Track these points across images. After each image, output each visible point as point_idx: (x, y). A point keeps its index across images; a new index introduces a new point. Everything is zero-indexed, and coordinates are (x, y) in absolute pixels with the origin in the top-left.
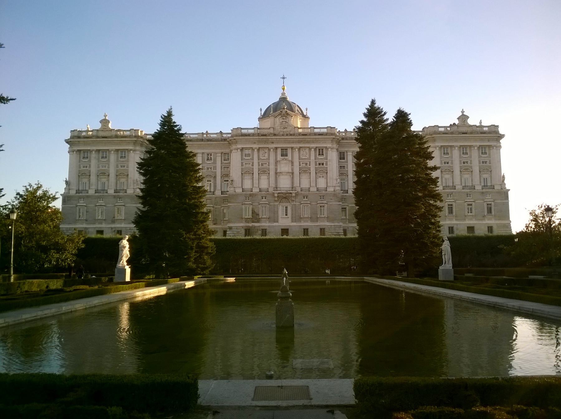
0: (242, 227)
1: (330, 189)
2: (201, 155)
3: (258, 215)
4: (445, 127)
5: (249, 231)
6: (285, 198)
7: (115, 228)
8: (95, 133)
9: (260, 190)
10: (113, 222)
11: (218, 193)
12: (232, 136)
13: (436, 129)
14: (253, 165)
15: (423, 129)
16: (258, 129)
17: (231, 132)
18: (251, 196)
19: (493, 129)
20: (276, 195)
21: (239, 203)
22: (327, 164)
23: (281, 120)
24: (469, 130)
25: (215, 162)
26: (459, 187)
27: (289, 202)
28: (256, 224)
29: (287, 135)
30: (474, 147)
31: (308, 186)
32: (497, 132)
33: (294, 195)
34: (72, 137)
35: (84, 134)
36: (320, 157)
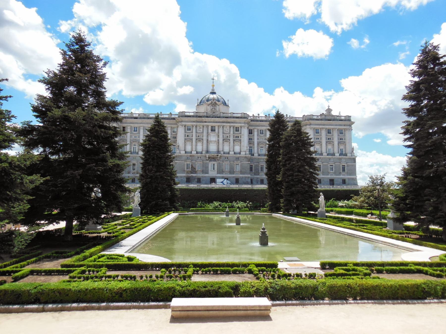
1: (243, 153)
3: (195, 169)
4: (318, 116)
5: (189, 180)
6: (214, 158)
9: (197, 153)
12: (179, 117)
13: (311, 117)
14: (192, 136)
15: (303, 116)
16: (196, 112)
17: (178, 114)
18: (190, 156)
19: (347, 118)
20: (207, 156)
22: (241, 137)
23: (212, 108)
24: (333, 118)
26: (325, 154)
27: (216, 161)
28: (194, 175)
29: (215, 117)
30: (335, 129)
32: (349, 120)
33: (219, 156)
36: (236, 132)
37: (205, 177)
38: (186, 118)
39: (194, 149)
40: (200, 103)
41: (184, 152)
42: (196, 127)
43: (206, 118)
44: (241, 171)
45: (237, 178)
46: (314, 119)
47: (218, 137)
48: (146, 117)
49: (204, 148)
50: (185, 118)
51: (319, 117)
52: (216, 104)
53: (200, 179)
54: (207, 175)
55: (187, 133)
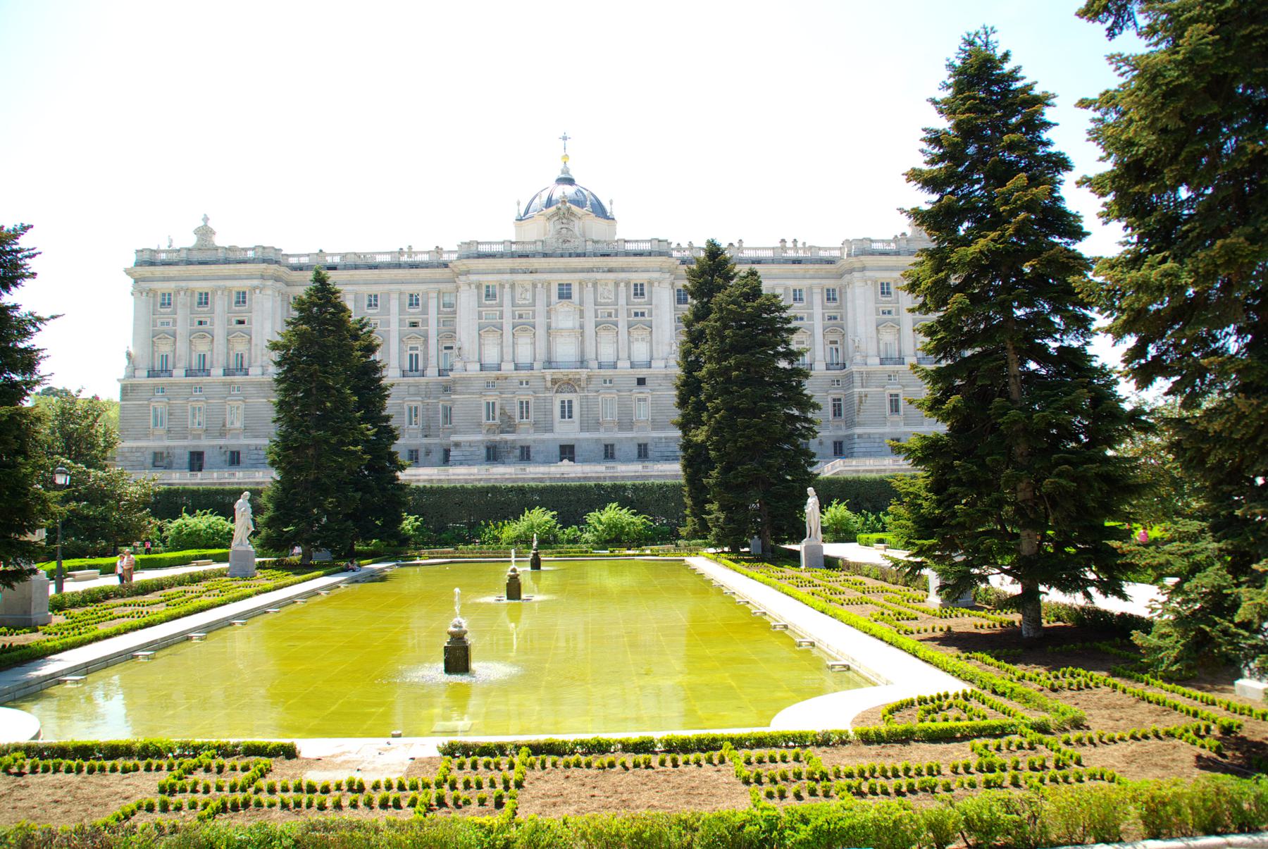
0: (482, 442)
2: (397, 296)
3: (510, 417)
4: (888, 242)
6: (568, 384)
7: (227, 446)
8: (183, 255)
10: (222, 434)
11: (432, 372)
12: (459, 258)
13: (866, 246)
16: (512, 243)
17: (456, 249)
18: (494, 377)
20: (549, 378)
21: (473, 393)
23: (559, 227)
25: (425, 312)
27: (576, 391)
29: (570, 255)
31: (612, 359)
33: (584, 376)
34: (139, 264)
35: (163, 256)
36: (636, 300)
37: (543, 441)
38: (481, 260)
39: (508, 357)
40: (527, 212)
41: (477, 366)
42: (513, 286)
43: (543, 260)
44: (653, 421)
45: (641, 442)
46: (873, 253)
47: (582, 317)
48: (363, 262)
49: (537, 350)
50: (476, 261)
51: (893, 246)
52: (572, 214)
53: (528, 447)
54: (547, 436)
55: (487, 306)
